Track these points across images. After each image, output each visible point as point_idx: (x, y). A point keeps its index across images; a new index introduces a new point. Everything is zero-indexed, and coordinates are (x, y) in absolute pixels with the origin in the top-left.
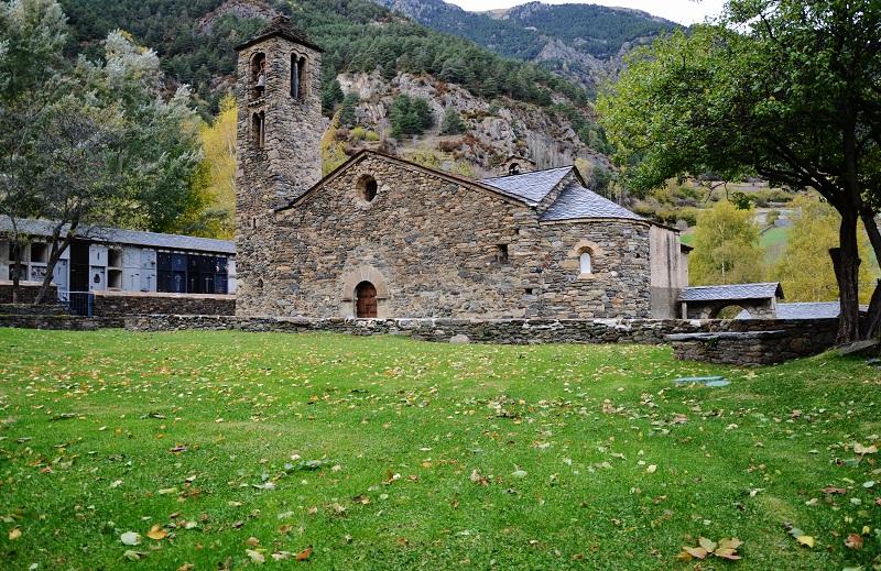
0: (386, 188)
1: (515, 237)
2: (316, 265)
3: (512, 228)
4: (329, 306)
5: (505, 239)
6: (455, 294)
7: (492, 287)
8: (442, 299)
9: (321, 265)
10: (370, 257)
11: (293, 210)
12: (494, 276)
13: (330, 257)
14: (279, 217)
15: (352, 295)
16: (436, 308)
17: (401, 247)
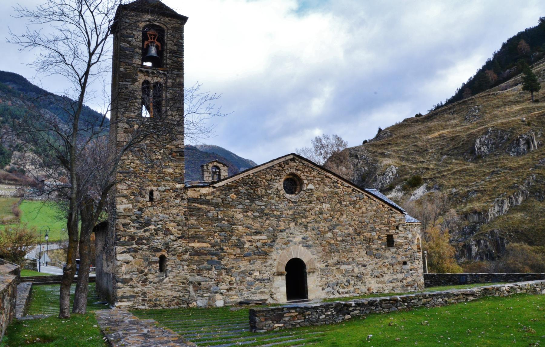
0: (311, 186)
1: (397, 231)
2: (244, 243)
3: (394, 226)
4: (258, 280)
6: (365, 266)
7: (386, 261)
8: (356, 270)
9: (249, 244)
10: (299, 239)
11: (211, 189)
12: (388, 254)
13: (258, 237)
14: (191, 194)
15: (283, 269)
16: (352, 276)
17: (325, 232)
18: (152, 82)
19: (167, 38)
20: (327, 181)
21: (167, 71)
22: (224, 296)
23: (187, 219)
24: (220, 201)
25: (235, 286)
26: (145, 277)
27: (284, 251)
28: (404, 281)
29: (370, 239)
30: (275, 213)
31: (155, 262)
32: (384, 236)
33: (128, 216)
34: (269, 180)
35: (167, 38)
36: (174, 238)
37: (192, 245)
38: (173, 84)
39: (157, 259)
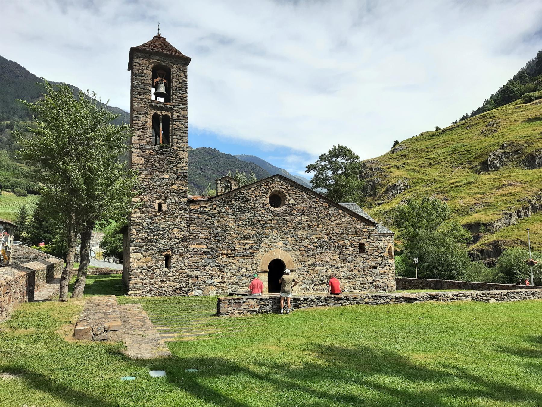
0: (293, 201)
1: (368, 240)
5: (364, 240)
8: (329, 270)
9: (239, 246)
10: (280, 244)
12: (359, 259)
14: (192, 207)
15: (266, 268)
18: (161, 115)
19: (173, 76)
20: (306, 196)
21: (173, 106)
22: (217, 288)
23: (188, 226)
24: (216, 212)
25: (226, 280)
26: (152, 272)
27: (268, 253)
28: (374, 283)
29: (343, 246)
30: (261, 222)
31: (162, 260)
32: (356, 244)
33: (141, 223)
34: (257, 196)
35: (173, 76)
36: (178, 241)
37: (193, 246)
38: (178, 116)
39: (163, 257)
